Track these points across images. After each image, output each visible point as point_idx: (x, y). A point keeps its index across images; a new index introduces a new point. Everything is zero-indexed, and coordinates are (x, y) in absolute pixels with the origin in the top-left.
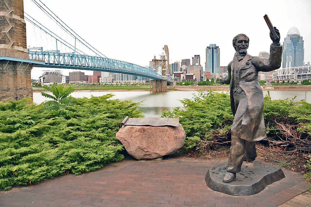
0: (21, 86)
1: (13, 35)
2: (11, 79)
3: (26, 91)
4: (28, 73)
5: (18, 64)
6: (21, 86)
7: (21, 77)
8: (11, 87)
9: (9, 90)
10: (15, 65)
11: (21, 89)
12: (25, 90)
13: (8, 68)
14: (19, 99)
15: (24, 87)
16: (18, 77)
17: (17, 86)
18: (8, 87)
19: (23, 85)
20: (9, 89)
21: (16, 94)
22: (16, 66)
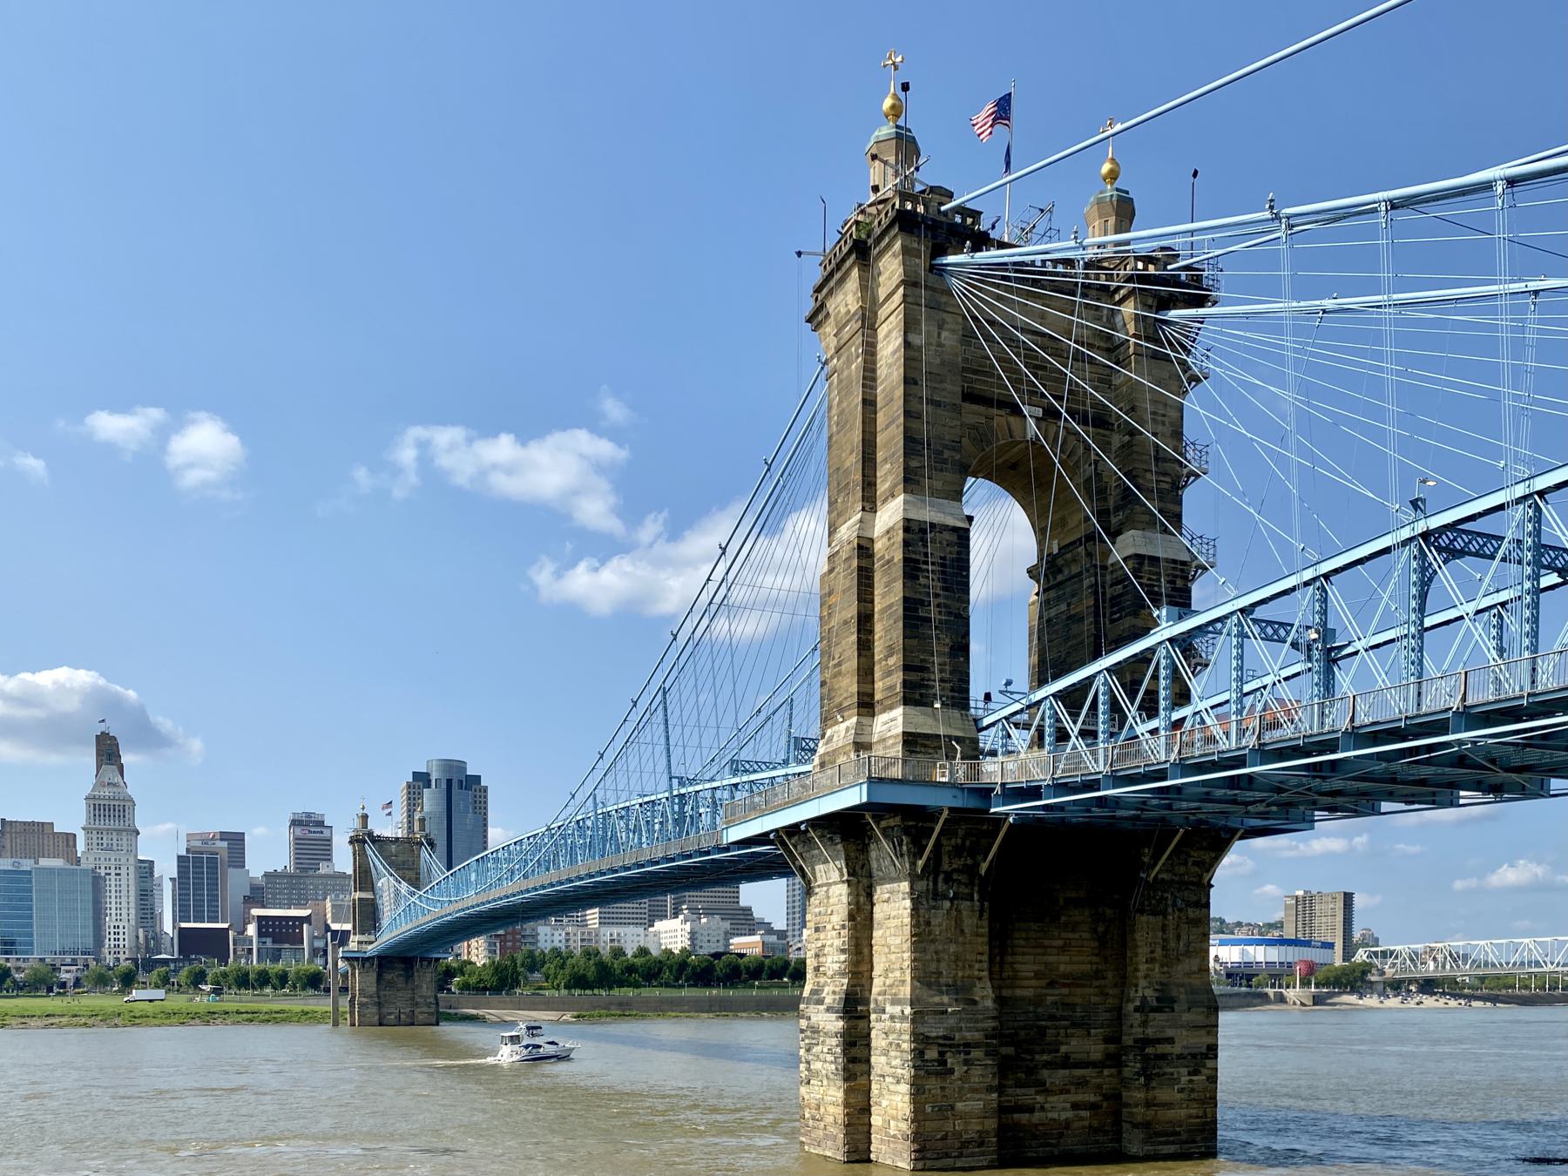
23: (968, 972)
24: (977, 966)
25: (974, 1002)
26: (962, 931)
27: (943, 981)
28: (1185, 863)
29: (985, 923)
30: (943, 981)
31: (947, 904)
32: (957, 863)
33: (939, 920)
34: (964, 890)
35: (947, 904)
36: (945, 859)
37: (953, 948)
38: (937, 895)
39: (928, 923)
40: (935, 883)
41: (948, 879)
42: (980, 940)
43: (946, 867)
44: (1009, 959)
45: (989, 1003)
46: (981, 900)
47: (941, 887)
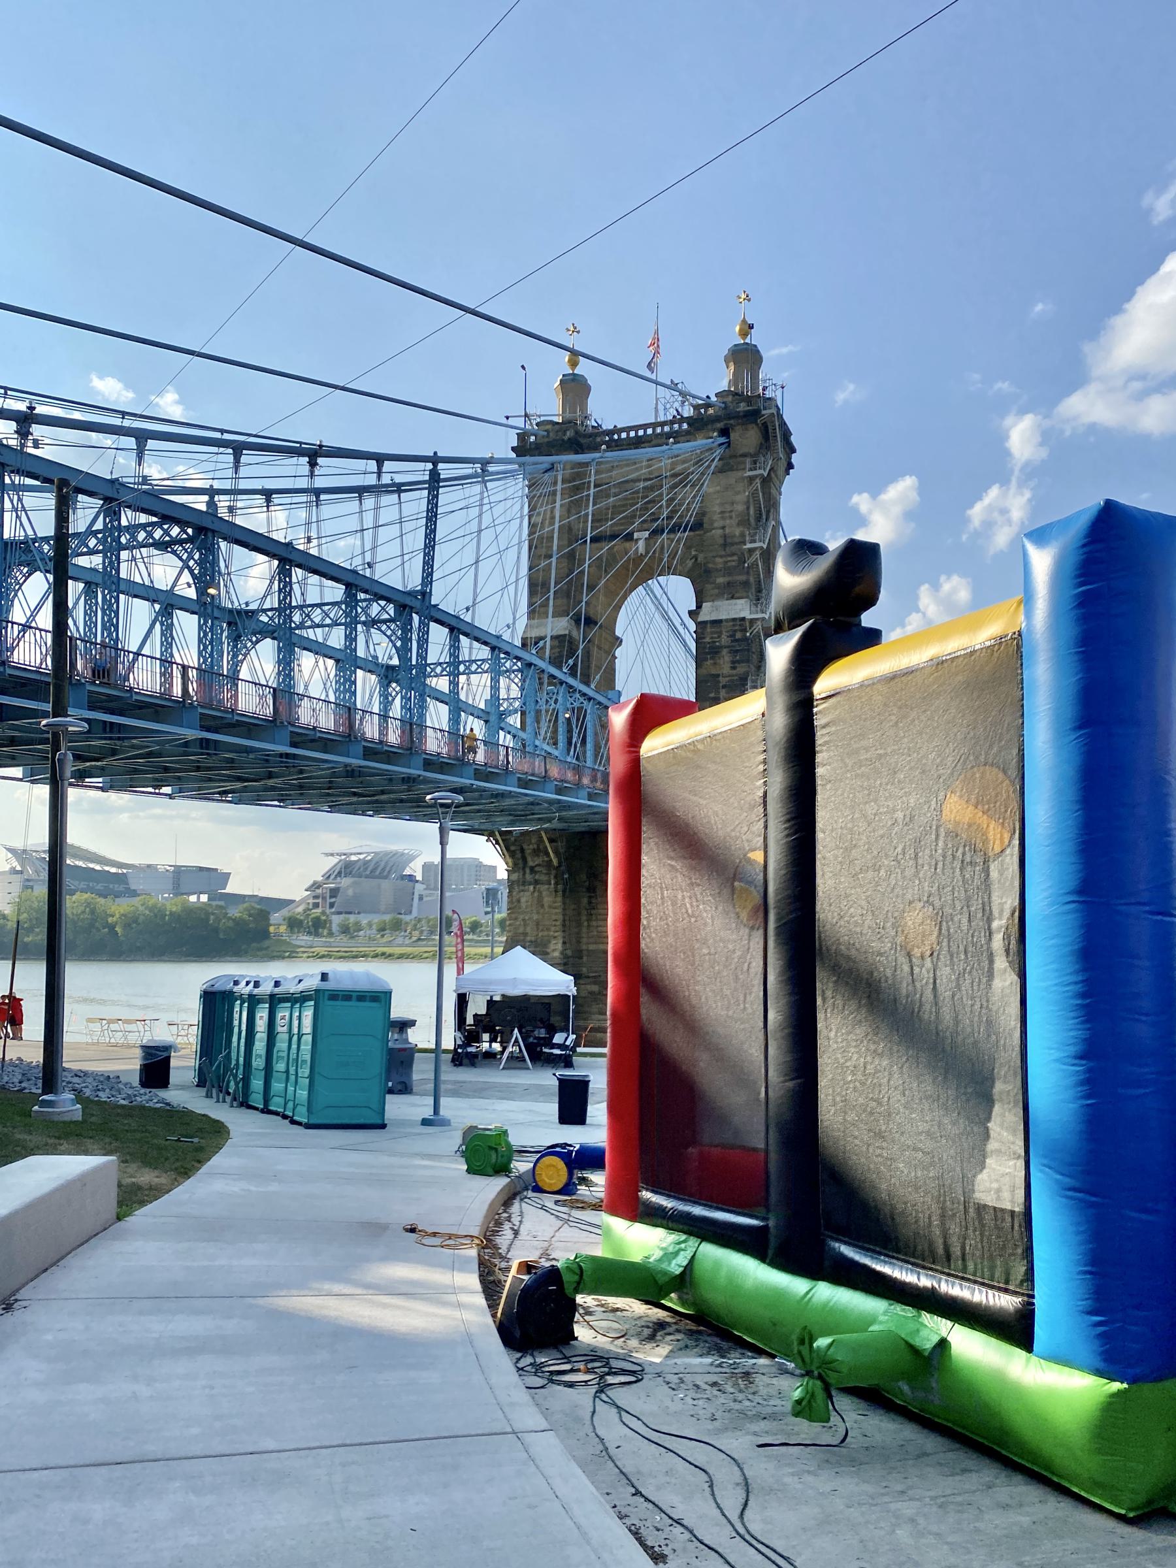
23: (546, 933)
24: (553, 928)
25: (547, 954)
26: (542, 906)
27: (529, 938)
29: (559, 899)
30: (529, 938)
31: (531, 888)
32: (538, 861)
33: (526, 898)
34: (544, 878)
35: (531, 888)
36: (529, 859)
37: (535, 917)
38: (524, 884)
39: (519, 901)
40: (524, 874)
41: (532, 869)
42: (555, 911)
43: (531, 863)
44: (594, 923)
45: (556, 954)
46: (556, 884)
47: (528, 877)
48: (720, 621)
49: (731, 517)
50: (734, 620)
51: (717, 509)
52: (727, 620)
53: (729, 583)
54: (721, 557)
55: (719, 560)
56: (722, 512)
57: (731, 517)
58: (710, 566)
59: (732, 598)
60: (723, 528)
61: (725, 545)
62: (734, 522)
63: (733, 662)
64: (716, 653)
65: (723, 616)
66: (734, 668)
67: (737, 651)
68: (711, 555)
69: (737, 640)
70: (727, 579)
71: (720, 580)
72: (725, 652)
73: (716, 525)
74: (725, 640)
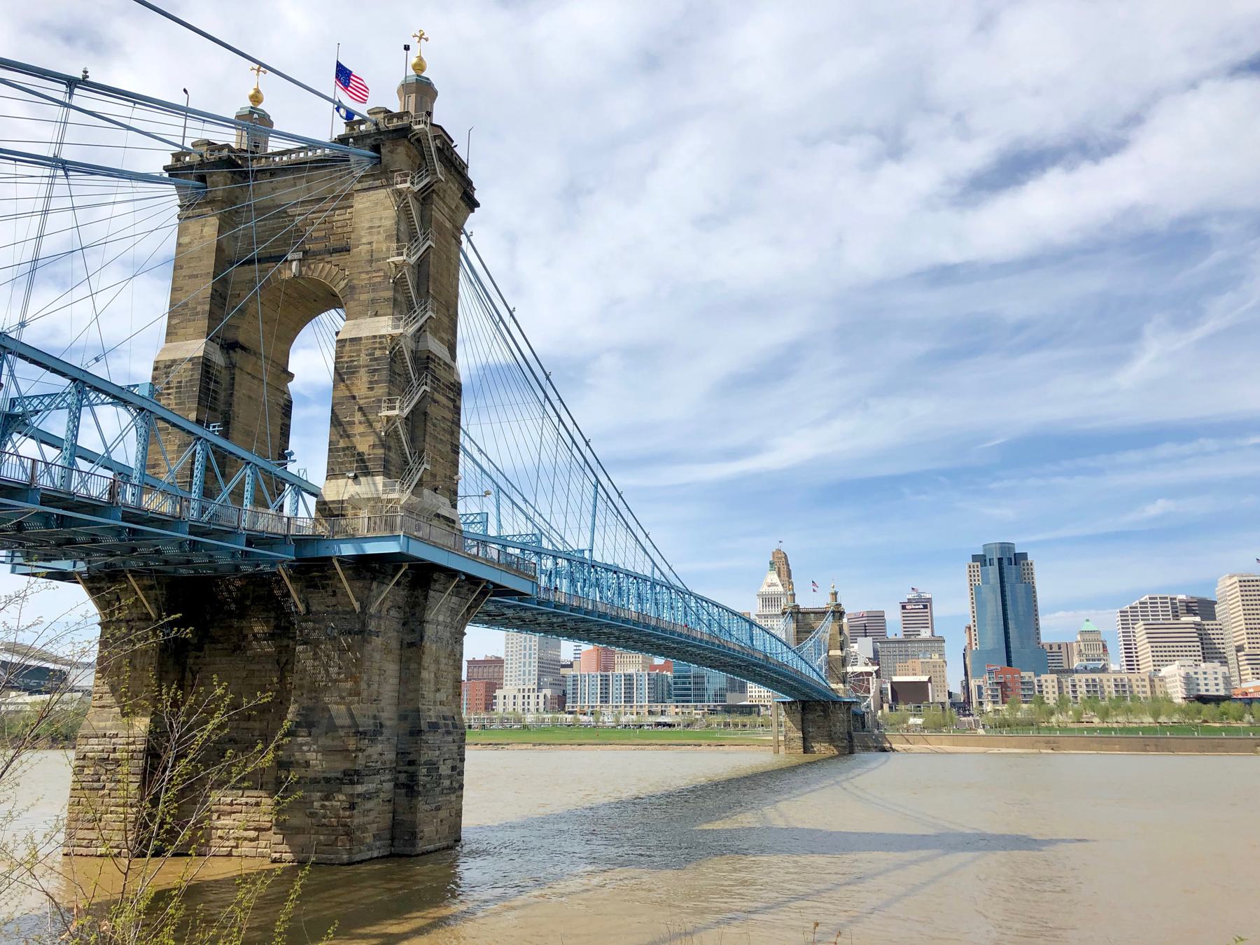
0: (432, 713)
1: (419, 432)
2: (392, 668)
3: (450, 738)
4: (458, 636)
5: (437, 586)
6: (432, 713)
7: (437, 661)
8: (388, 715)
9: (381, 734)
10: (419, 592)
11: (434, 727)
12: (448, 733)
13: (388, 604)
14: (424, 786)
15: (445, 718)
16: (427, 660)
17: (418, 710)
18: (375, 717)
19: (442, 703)
20: (381, 725)
21: (411, 757)
22: (426, 598)
28: (334, 593)
48: (360, 339)
49: (379, 233)
50: (375, 337)
51: (367, 225)
52: (367, 338)
53: (373, 301)
54: (367, 273)
55: (364, 276)
56: (371, 228)
57: (379, 233)
58: (355, 282)
59: (376, 315)
60: (370, 243)
61: (371, 261)
62: (382, 237)
63: (371, 382)
64: (353, 373)
65: (364, 333)
66: (371, 389)
67: (375, 370)
68: (356, 270)
69: (376, 359)
70: (371, 295)
71: (364, 297)
72: (363, 371)
73: (364, 240)
74: (364, 359)
